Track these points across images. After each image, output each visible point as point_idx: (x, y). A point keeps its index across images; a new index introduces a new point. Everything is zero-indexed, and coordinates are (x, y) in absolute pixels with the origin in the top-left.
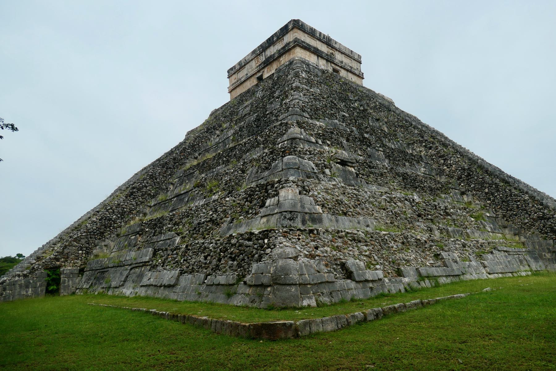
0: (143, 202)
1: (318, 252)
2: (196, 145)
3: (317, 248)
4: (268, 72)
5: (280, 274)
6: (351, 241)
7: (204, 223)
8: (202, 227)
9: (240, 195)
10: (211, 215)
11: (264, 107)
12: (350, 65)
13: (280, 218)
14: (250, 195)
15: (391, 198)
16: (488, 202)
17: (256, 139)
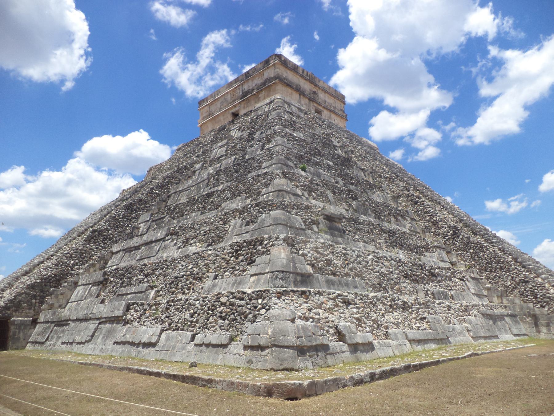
0: (105, 247)
1: (312, 314)
2: (165, 186)
3: (310, 310)
4: (244, 108)
5: (278, 335)
6: (342, 303)
7: (183, 276)
8: (181, 281)
9: (224, 249)
10: (191, 268)
11: (244, 150)
12: (334, 105)
13: (272, 278)
14: (237, 249)
15: (378, 258)
16: (473, 262)
17: (237, 186)
